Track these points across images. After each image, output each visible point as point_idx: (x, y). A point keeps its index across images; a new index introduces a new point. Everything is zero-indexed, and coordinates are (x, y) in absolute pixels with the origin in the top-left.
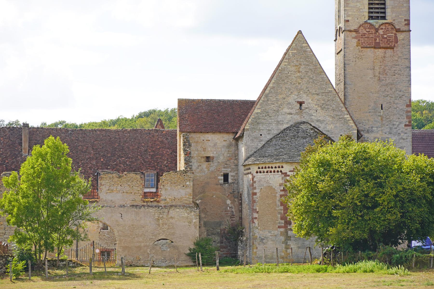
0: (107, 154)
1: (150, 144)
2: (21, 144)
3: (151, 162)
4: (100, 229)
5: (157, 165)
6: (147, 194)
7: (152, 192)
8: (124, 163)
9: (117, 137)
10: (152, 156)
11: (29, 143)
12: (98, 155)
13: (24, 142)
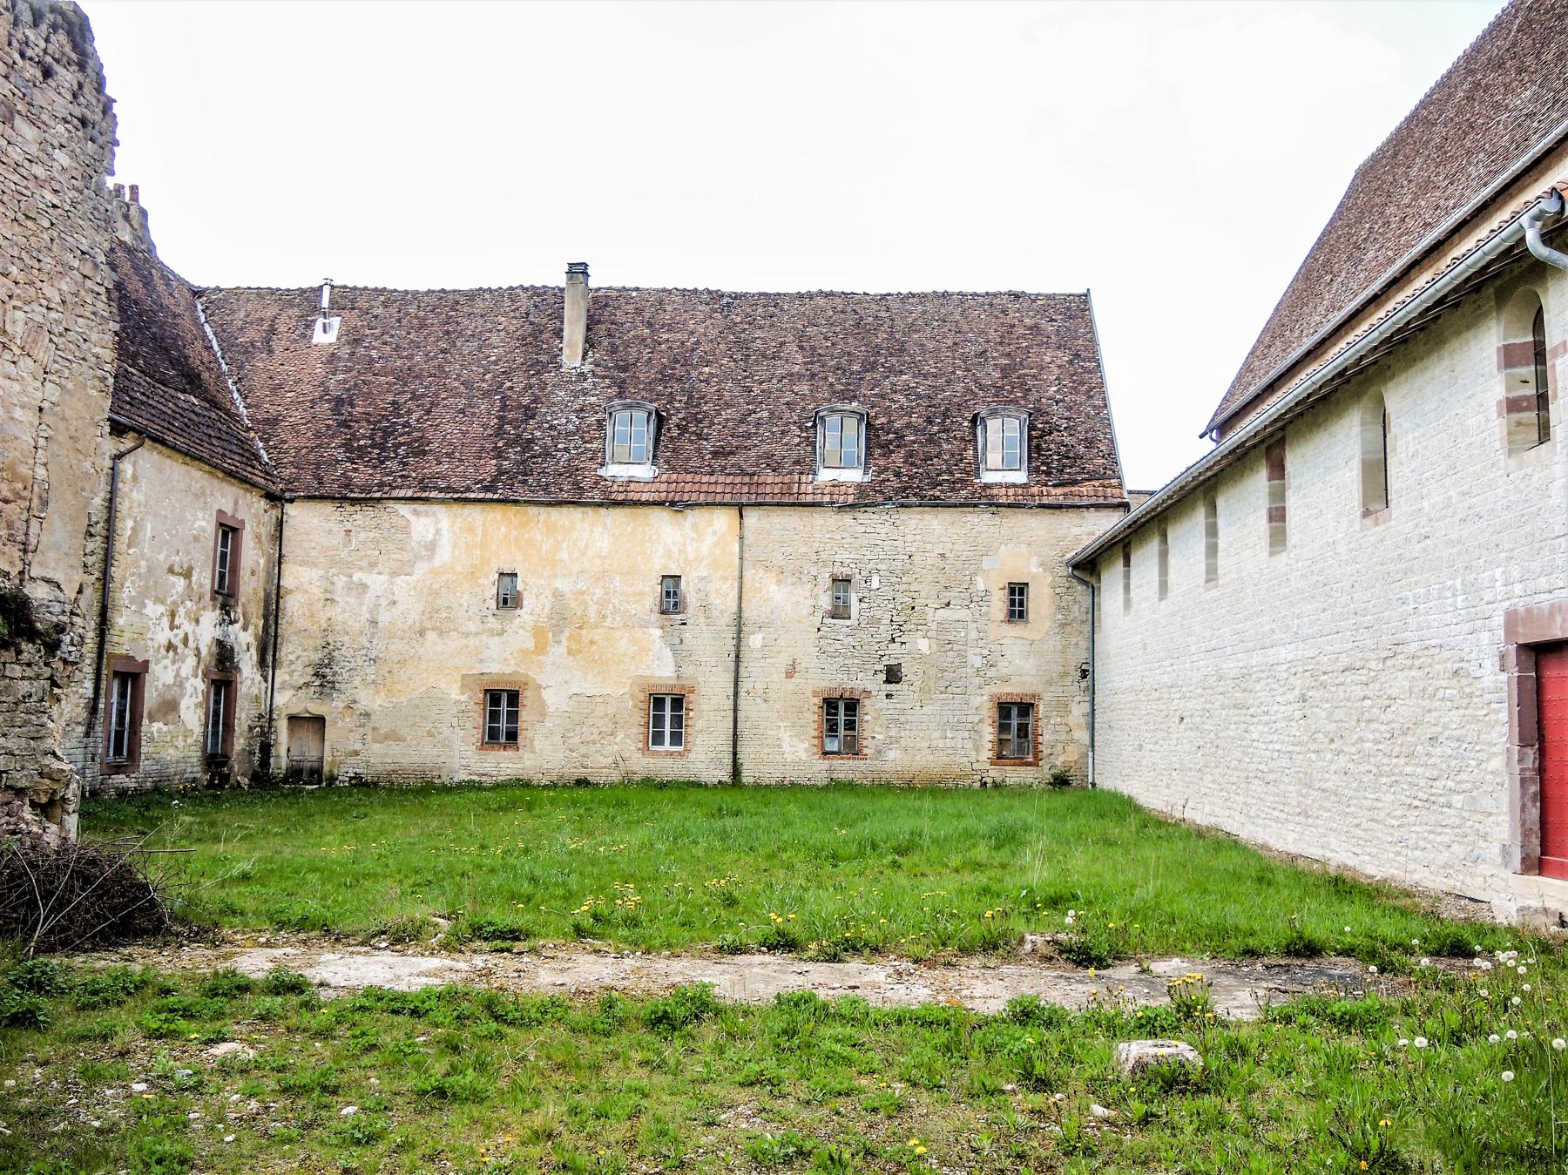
0: (850, 362)
1: (993, 335)
2: (558, 333)
3: (1002, 388)
4: (819, 614)
5: (1024, 398)
6: (995, 491)
7: (1014, 486)
8: (908, 391)
9: (883, 314)
10: (1006, 372)
11: (589, 329)
12: (816, 368)
13: (571, 322)
